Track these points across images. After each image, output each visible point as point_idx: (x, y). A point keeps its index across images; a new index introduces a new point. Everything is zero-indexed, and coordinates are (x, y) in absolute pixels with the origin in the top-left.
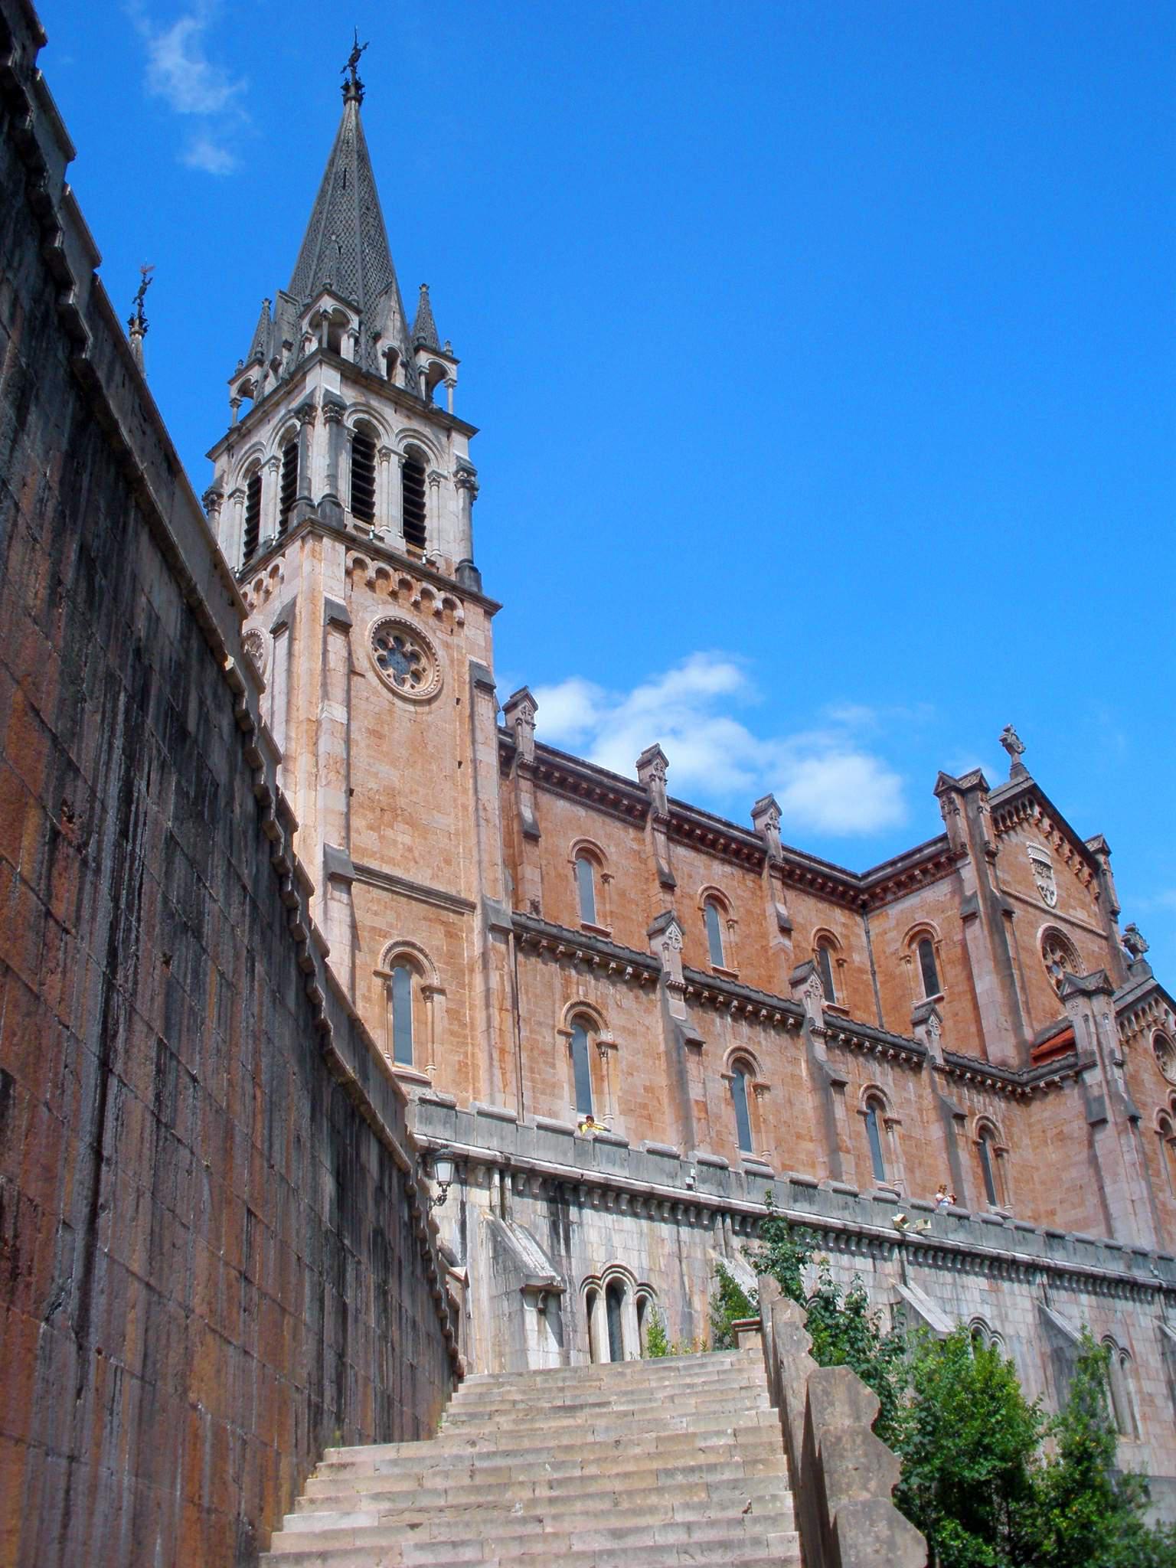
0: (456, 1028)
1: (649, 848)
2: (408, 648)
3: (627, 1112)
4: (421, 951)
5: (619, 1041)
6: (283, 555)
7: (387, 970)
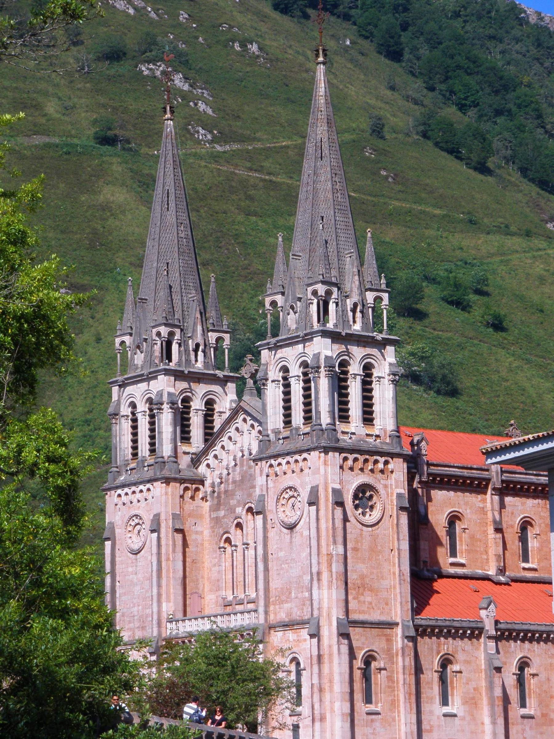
0: (390, 684)
1: (489, 505)
2: (368, 494)
3: (465, 702)
4: (376, 652)
5: (463, 669)
6: (309, 454)
7: (363, 666)
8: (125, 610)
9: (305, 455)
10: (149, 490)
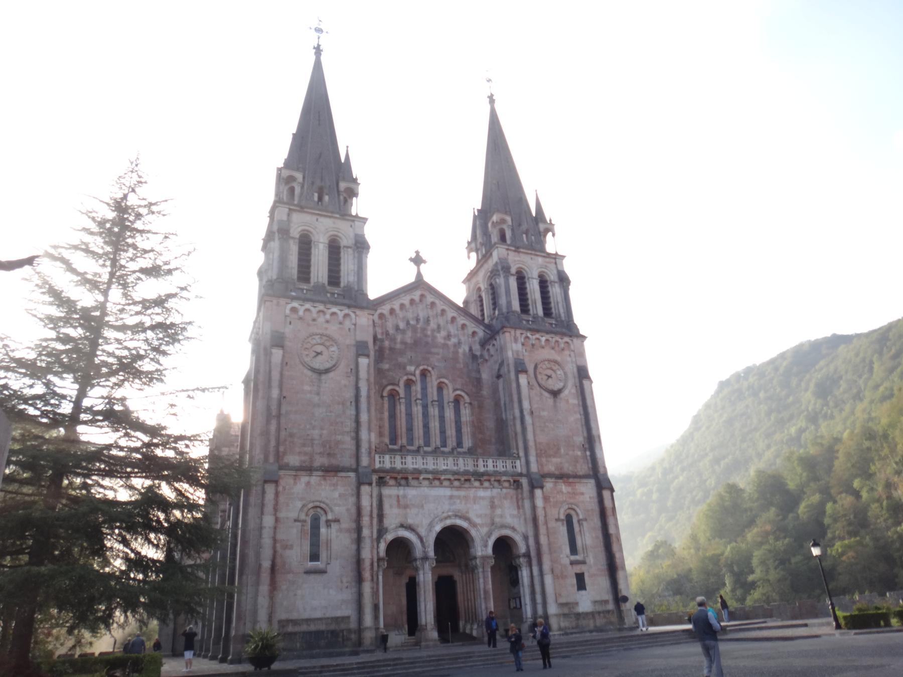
8: (295, 431)
9: (567, 339)
10: (346, 316)
